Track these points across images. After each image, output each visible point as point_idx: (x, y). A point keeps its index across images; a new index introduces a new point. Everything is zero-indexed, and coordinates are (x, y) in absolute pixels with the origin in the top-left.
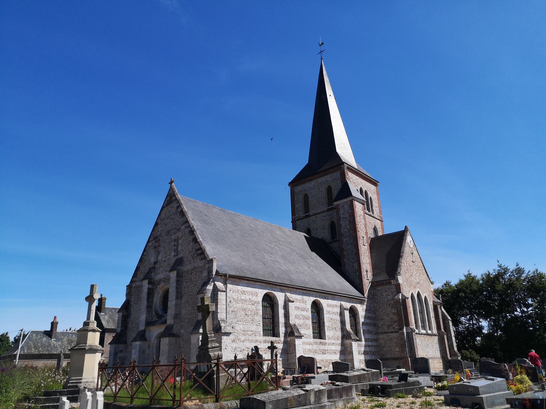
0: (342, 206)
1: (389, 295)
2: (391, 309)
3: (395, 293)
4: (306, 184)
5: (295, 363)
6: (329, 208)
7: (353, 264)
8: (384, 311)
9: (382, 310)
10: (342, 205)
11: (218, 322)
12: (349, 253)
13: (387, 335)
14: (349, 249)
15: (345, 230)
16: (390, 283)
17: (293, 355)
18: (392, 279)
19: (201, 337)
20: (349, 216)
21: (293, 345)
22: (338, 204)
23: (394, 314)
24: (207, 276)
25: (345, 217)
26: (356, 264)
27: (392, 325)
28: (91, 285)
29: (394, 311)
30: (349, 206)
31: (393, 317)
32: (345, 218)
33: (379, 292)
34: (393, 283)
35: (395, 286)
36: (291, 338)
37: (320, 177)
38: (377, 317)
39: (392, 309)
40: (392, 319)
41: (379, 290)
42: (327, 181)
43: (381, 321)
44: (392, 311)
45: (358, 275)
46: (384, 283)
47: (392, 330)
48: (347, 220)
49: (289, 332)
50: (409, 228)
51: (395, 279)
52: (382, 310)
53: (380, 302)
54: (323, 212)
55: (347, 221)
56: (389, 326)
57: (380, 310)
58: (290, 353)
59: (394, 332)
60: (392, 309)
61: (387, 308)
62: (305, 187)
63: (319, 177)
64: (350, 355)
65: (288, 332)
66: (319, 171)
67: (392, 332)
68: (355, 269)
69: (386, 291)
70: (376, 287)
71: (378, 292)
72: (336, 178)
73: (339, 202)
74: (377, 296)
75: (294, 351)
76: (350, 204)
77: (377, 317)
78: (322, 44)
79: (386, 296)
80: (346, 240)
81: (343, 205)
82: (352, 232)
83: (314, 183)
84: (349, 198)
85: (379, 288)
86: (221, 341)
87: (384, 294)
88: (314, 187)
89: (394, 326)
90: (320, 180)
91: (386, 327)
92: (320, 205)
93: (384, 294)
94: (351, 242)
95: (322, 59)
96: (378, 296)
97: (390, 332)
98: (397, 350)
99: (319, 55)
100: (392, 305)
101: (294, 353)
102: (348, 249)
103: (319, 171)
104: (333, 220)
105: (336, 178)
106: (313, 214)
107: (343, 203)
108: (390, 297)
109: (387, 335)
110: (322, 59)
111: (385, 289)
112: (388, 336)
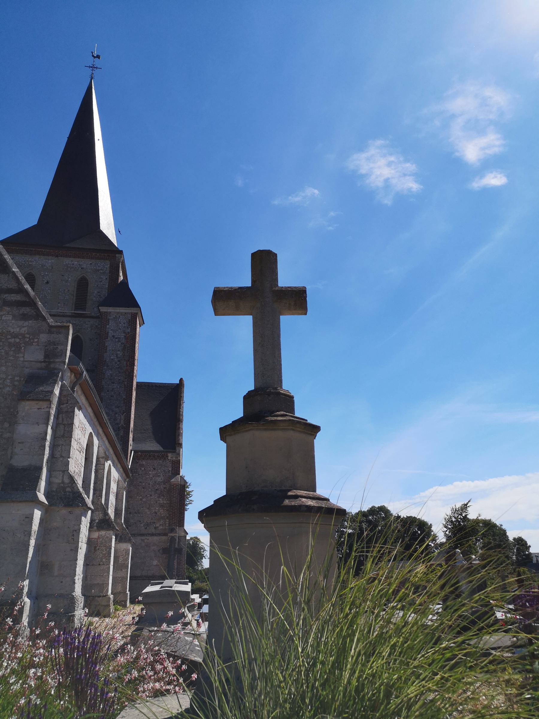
0: (114, 318)
1: (159, 476)
2: (158, 497)
3: (170, 474)
4: (37, 257)
5: (103, 584)
6: (76, 312)
7: (117, 415)
8: (144, 500)
9: (141, 497)
10: (114, 316)
11: (67, 481)
12: (112, 397)
13: (143, 538)
14: (113, 389)
15: (112, 358)
16: (165, 457)
17: (102, 567)
18: (170, 452)
19: (37, 514)
20: (125, 336)
21: (104, 548)
22: (107, 312)
23: (162, 506)
24: (41, 362)
25: (116, 337)
26: (123, 417)
27: (155, 523)
28: (254, 256)
29: (162, 502)
30: (128, 320)
31: (159, 510)
32: (116, 338)
33: (143, 469)
34: (169, 458)
35: (173, 463)
36: (103, 533)
37: (70, 257)
38: (130, 509)
39: (159, 497)
40: (156, 513)
41: (142, 465)
42: (82, 268)
43: (136, 515)
44: (158, 502)
45: (122, 434)
46: (154, 456)
47: (154, 531)
48: (119, 341)
49: (97, 521)
50: (186, 383)
51: (175, 452)
52: (141, 497)
53: (140, 484)
54: (64, 316)
55: (120, 343)
56: (147, 525)
57: (138, 497)
58: (93, 565)
59: (156, 534)
60: (159, 497)
61: (151, 495)
62: (31, 261)
63: (67, 256)
64: (121, 570)
65: (95, 520)
66: (68, 245)
67: (152, 535)
68: (118, 424)
69: (154, 469)
70: (139, 459)
71: (141, 469)
72: (102, 270)
73: (110, 310)
74: (137, 474)
75: (104, 560)
76: (130, 318)
77: (130, 509)
78: (98, 57)
79: (153, 477)
80: (111, 375)
81: (118, 316)
82: (125, 363)
83: (53, 261)
84: (132, 309)
85: (144, 463)
86: (76, 528)
87: (150, 472)
88: (52, 268)
89: (157, 525)
90: (67, 261)
91: (142, 525)
92: (59, 303)
93: (150, 472)
94: (120, 380)
95: (92, 78)
96: (139, 475)
97: (149, 534)
98: (155, 562)
99: (89, 71)
100: (161, 491)
101: (104, 564)
102: (111, 389)
103: (68, 245)
104: (79, 334)
105: (102, 270)
106: (70, 314)
107: (118, 313)
108: (160, 478)
109: (141, 539)
110: (92, 78)
111: (153, 465)
112: (143, 540)
